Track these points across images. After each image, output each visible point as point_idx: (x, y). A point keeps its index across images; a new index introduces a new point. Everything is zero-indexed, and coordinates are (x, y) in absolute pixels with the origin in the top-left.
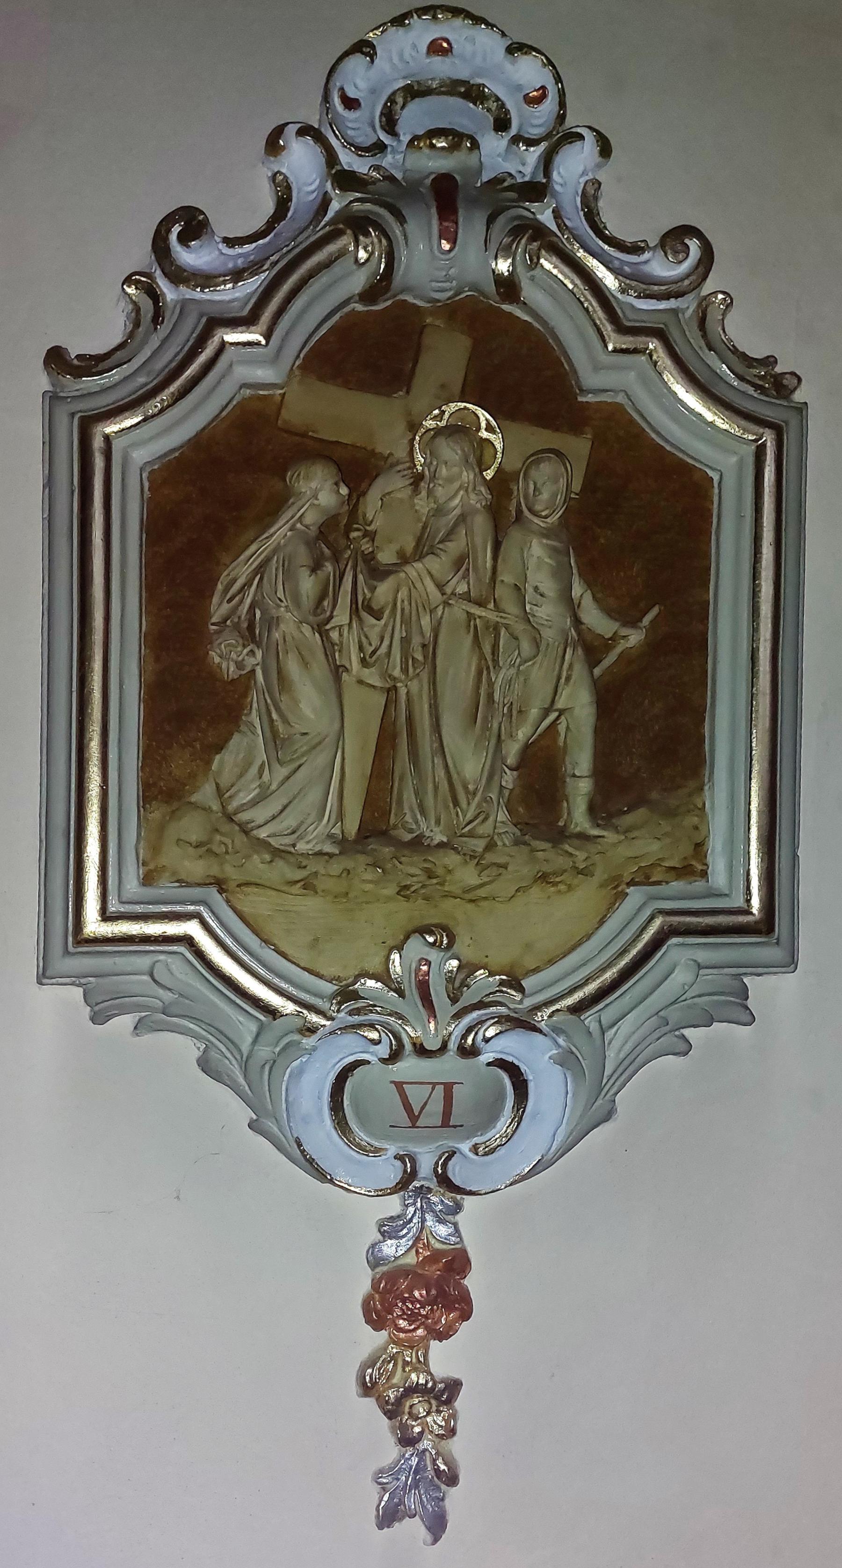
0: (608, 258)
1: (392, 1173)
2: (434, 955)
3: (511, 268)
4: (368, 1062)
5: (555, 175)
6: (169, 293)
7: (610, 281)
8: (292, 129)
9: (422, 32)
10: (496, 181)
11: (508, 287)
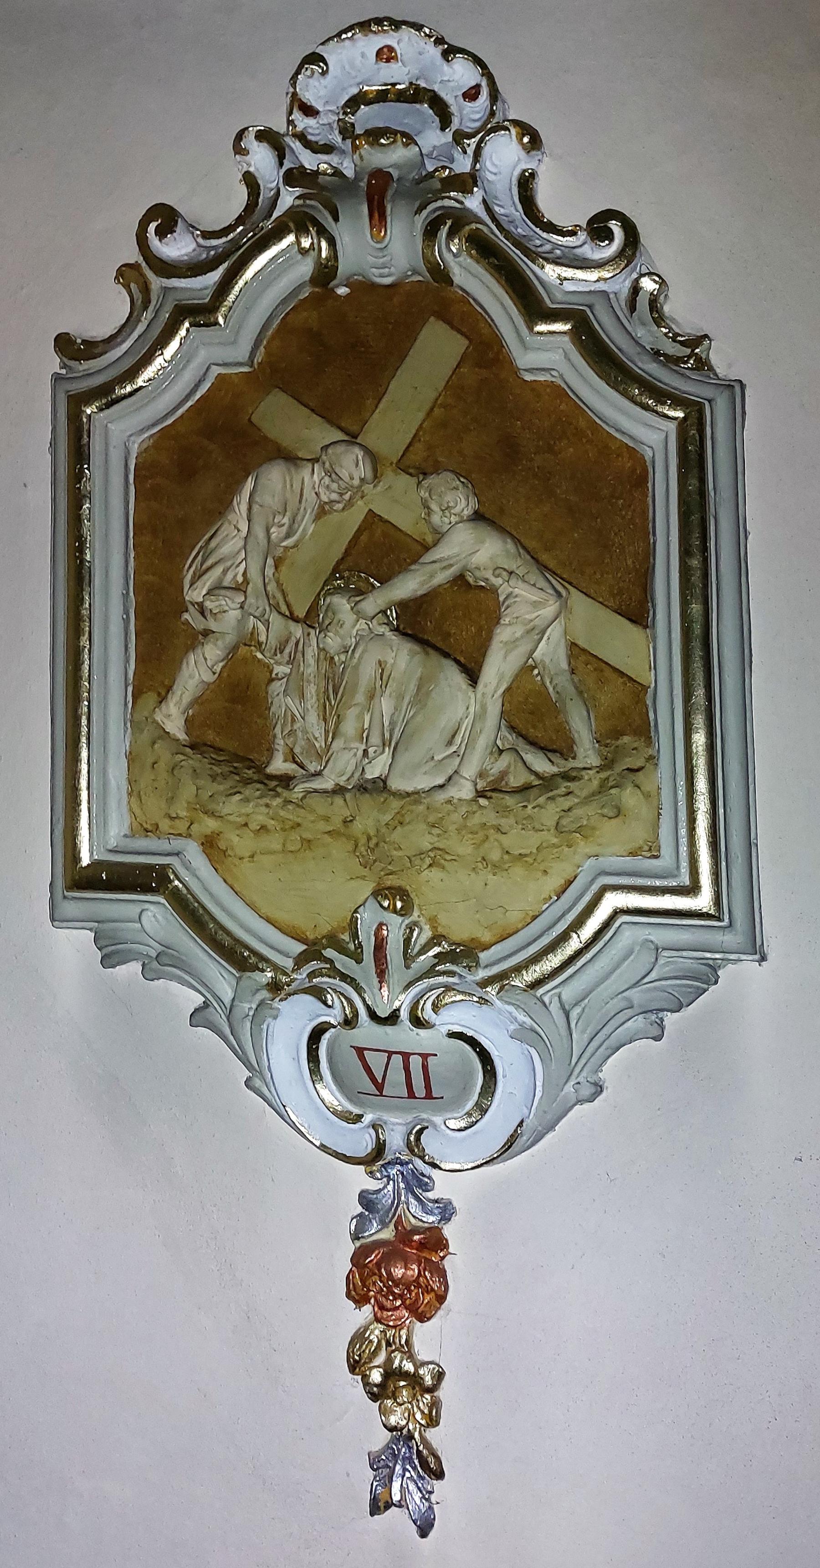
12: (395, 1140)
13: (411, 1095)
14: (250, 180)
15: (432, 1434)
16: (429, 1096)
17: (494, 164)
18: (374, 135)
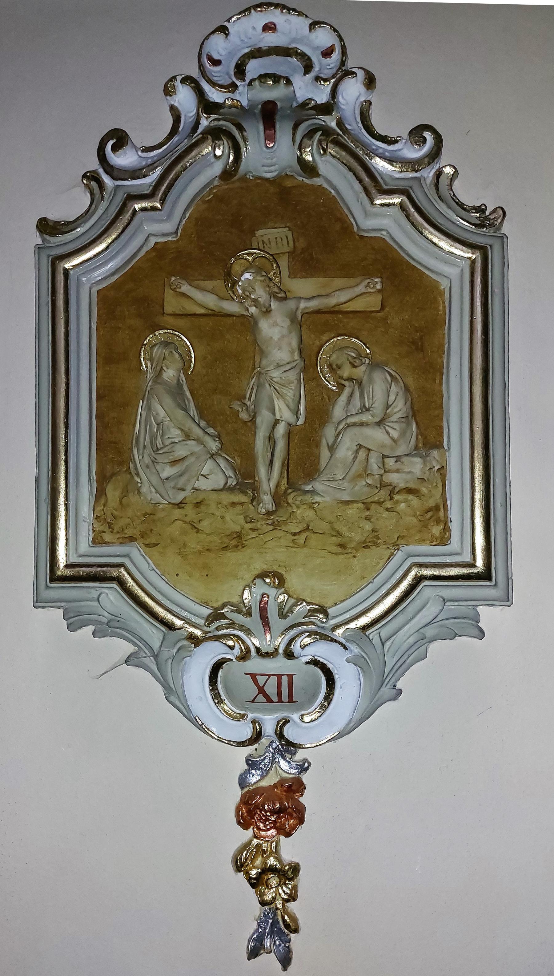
1: (246, 732)
2: (272, 592)
4: (230, 660)
9: (259, 19)
10: (304, 105)
12: (269, 729)
13: (280, 700)
15: (291, 906)
16: (291, 699)
18: (263, 77)
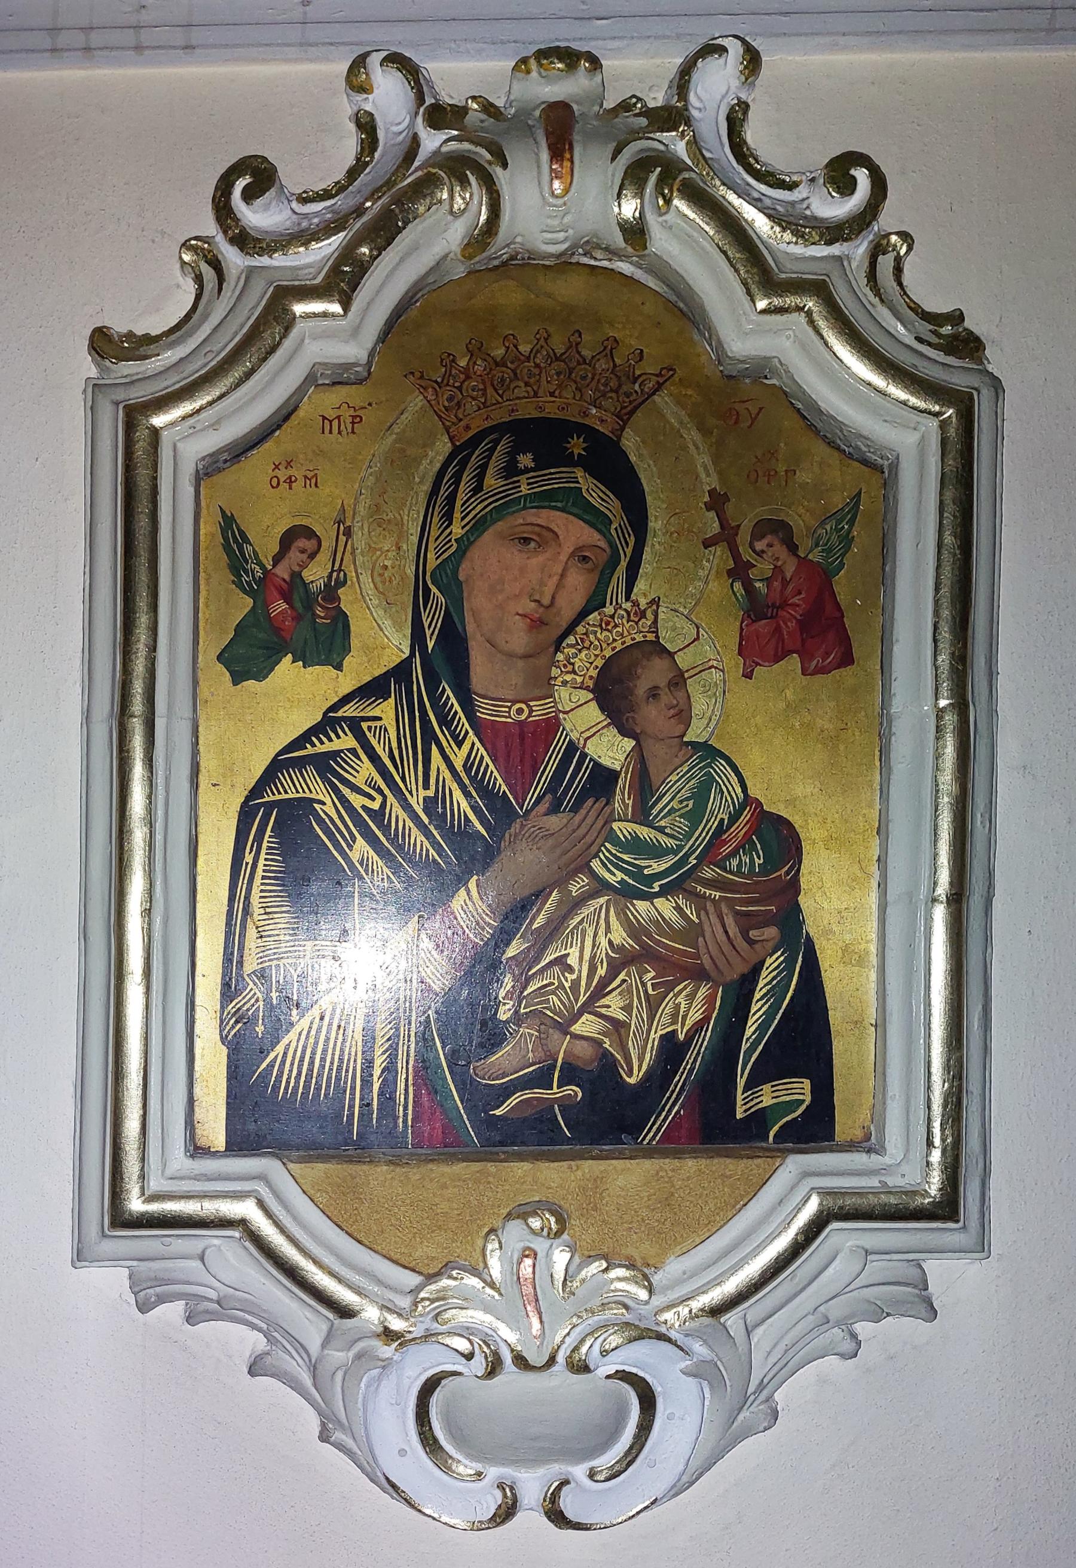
0: (756, 195)
3: (637, 214)
5: (692, 98)
6: (233, 257)
7: (760, 223)
8: (375, 60)
11: (636, 232)
14: (366, 125)
17: (699, 98)
